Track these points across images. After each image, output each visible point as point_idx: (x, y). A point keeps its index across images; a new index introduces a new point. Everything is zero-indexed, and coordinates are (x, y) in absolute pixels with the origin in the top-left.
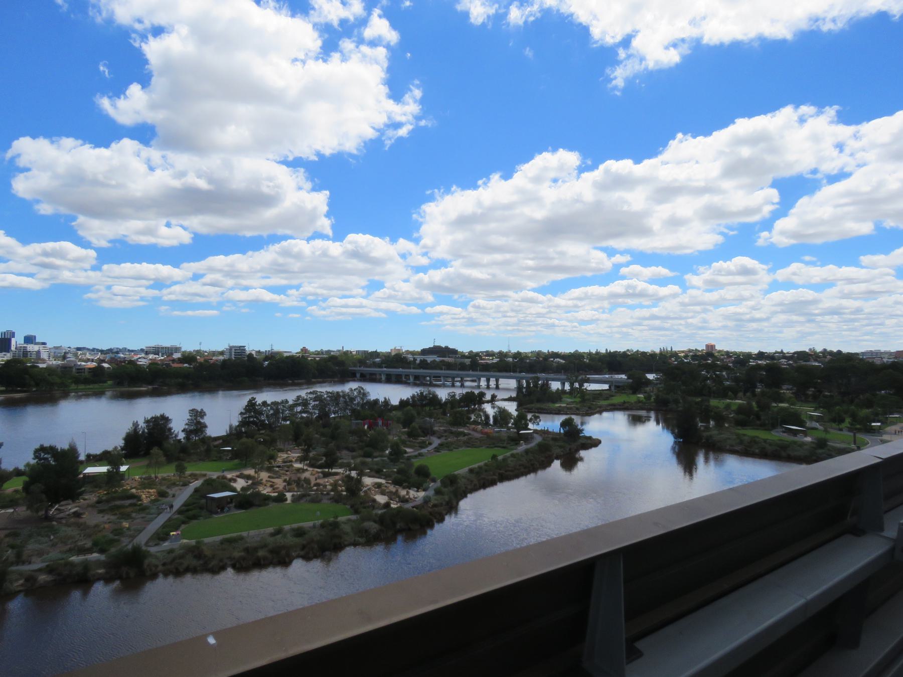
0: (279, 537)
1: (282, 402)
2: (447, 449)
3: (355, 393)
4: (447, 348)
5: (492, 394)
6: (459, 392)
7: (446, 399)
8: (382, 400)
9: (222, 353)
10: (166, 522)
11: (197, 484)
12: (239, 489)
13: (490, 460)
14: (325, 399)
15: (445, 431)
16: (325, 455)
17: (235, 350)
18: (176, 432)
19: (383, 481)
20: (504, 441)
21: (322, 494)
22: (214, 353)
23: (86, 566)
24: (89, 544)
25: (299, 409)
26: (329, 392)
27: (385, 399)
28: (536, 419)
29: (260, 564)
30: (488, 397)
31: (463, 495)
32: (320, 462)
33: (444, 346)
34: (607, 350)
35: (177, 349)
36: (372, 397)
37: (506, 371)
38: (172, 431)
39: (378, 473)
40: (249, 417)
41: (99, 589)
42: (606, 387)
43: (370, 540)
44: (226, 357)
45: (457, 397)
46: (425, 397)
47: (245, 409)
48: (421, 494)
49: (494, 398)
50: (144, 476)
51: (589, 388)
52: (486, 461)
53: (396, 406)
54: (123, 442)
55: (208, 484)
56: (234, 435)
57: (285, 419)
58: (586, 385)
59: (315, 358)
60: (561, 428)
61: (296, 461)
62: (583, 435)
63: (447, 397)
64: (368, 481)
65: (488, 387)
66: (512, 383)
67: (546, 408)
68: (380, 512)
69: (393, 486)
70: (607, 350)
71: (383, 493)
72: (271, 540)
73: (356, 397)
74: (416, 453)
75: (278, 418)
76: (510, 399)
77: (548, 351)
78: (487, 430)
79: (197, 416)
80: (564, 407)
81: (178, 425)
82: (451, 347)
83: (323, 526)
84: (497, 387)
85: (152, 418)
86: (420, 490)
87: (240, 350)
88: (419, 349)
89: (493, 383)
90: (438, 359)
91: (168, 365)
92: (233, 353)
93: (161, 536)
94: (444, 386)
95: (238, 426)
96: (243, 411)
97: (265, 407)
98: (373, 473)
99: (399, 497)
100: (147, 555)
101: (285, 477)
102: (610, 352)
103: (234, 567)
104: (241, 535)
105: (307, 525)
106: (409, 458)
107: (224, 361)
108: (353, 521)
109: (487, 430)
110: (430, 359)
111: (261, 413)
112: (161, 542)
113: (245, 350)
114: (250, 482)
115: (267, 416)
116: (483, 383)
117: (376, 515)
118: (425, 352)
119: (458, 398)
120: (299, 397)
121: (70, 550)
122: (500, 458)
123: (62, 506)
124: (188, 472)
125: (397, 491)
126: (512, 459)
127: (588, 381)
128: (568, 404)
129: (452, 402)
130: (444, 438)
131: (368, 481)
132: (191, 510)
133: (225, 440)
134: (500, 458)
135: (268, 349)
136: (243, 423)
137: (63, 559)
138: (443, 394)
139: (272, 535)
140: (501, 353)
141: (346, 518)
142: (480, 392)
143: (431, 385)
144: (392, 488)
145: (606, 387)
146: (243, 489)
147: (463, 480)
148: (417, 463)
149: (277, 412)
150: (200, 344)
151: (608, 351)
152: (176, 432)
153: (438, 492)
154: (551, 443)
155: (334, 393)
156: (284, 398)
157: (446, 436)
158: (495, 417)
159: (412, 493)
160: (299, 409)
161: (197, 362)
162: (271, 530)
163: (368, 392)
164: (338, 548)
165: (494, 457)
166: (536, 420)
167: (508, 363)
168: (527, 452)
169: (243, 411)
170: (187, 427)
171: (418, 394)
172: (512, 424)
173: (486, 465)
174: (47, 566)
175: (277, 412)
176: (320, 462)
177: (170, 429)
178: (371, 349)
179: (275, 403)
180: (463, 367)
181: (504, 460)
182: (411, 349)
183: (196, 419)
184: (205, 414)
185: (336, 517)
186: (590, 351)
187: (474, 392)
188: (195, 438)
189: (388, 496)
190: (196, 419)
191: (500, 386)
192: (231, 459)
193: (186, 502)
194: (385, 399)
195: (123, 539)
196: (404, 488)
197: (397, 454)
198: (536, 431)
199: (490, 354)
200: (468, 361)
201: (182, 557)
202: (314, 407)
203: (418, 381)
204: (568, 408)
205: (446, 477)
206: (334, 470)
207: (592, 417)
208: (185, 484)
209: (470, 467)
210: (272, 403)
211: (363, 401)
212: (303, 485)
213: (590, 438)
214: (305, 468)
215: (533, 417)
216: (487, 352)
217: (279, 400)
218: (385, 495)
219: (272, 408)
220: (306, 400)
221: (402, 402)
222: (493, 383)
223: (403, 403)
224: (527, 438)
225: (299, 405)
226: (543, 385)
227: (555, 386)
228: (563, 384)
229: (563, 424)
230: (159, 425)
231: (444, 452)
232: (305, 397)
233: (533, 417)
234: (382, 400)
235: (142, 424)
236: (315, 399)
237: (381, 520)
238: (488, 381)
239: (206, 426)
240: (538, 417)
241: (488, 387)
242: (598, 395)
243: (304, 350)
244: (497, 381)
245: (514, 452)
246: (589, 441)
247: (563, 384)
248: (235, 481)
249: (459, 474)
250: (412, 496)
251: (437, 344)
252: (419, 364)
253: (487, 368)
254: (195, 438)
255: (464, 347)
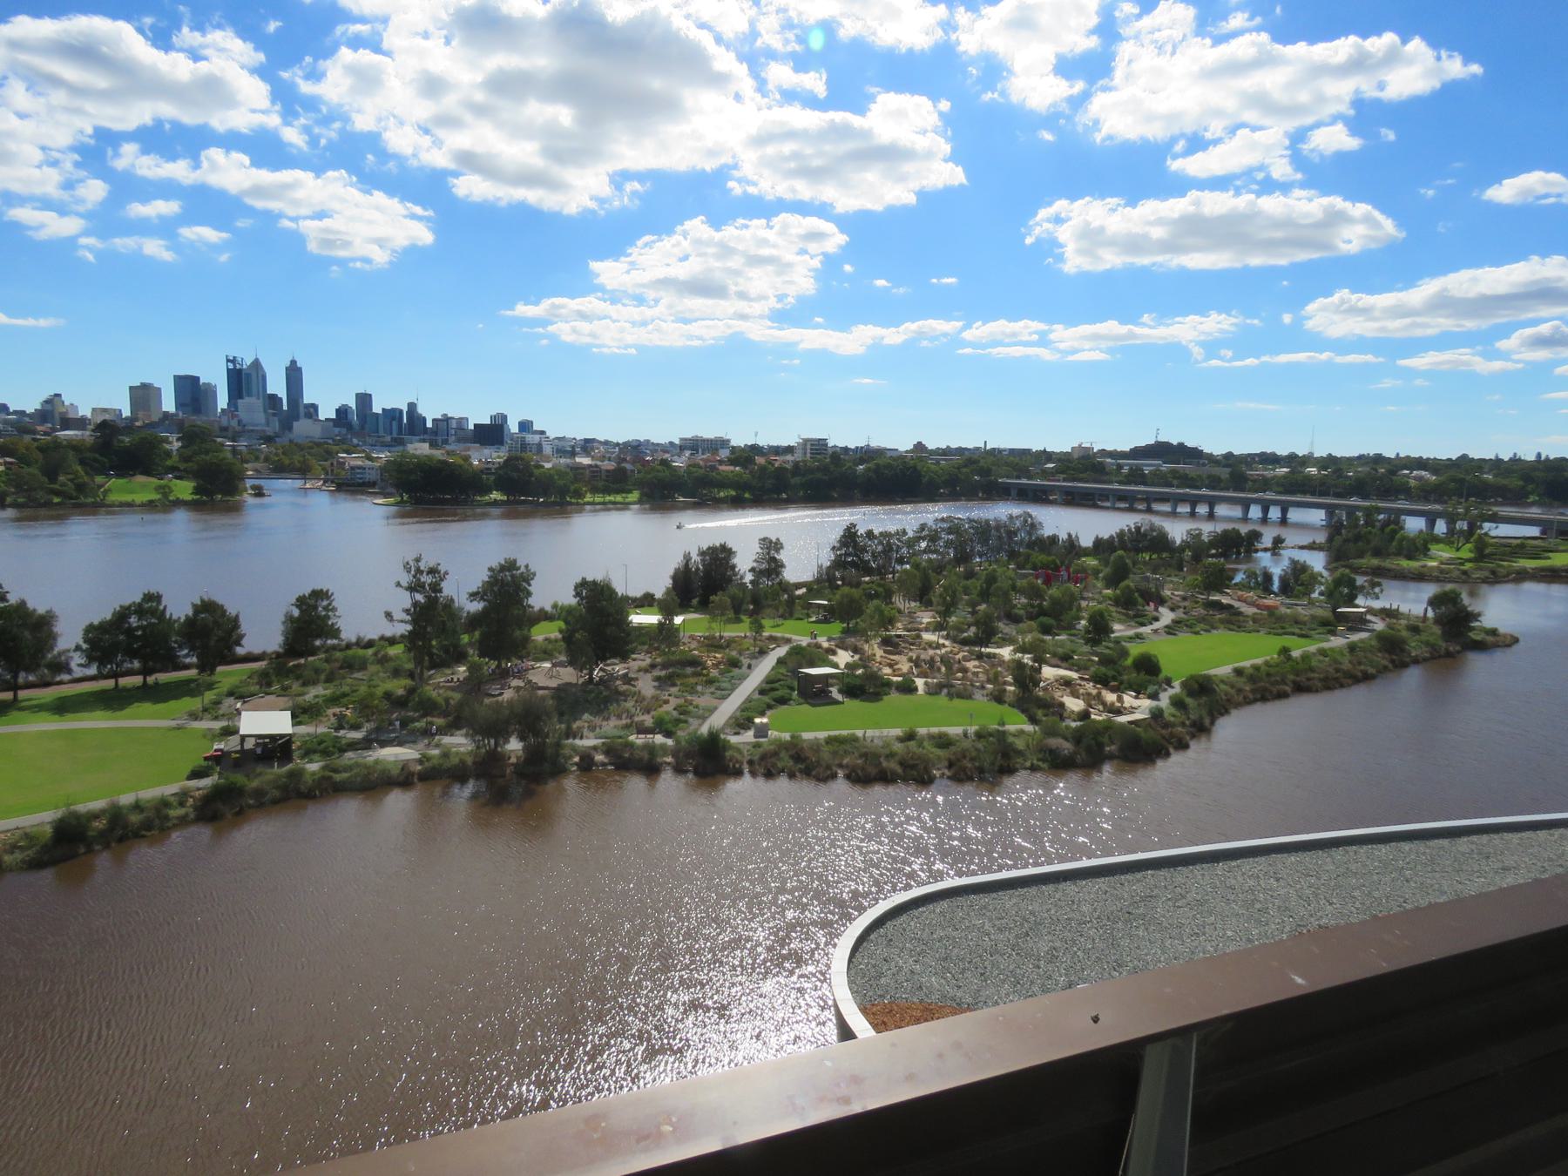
0: (912, 744)
1: (897, 533)
2: (1188, 630)
3: (1018, 524)
4: (1181, 445)
5: (1275, 535)
6: (1207, 529)
7: (1183, 541)
8: (1063, 536)
9: (789, 450)
10: (744, 702)
11: (782, 651)
12: (842, 666)
13: (1276, 656)
14: (966, 530)
15: (1184, 599)
16: (976, 624)
17: (812, 445)
18: (742, 572)
19: (1074, 675)
20: (1304, 623)
21: (972, 685)
22: (778, 451)
23: (651, 749)
24: (648, 720)
25: (923, 545)
26: (973, 521)
27: (1070, 535)
28: (1371, 590)
29: (886, 778)
30: (1267, 541)
31: (1223, 711)
32: (966, 634)
33: (1175, 443)
34: (1539, 455)
35: (723, 443)
36: (1047, 532)
37: (1304, 493)
38: (737, 570)
39: (1065, 660)
40: (846, 555)
41: (669, 782)
42: (1534, 531)
43: (1058, 764)
44: (798, 456)
45: (1205, 538)
46: (1145, 535)
47: (840, 541)
48: (1146, 703)
49: (1278, 542)
50: (707, 634)
51: (1493, 533)
52: (1268, 658)
53: (1086, 549)
54: (671, 582)
55: (797, 654)
56: (825, 581)
57: (901, 561)
58: (1487, 525)
59: (938, 462)
60: (1429, 609)
61: (927, 630)
62: (1477, 624)
63: (1185, 538)
64: (1048, 672)
65: (1264, 520)
66: (1317, 516)
67: (1393, 567)
68: (1074, 725)
69: (1091, 684)
70: (1539, 455)
71: (1075, 695)
72: (898, 747)
73: (1018, 529)
74: (1131, 633)
75: (890, 559)
76: (1312, 547)
77: (1398, 454)
78: (1270, 601)
79: (771, 547)
80: (1432, 567)
81: (745, 562)
82: (1190, 444)
83: (980, 735)
84: (1284, 521)
85: (709, 548)
86: (1141, 696)
87: (818, 446)
88: (1127, 449)
89: (1275, 513)
90: (1165, 467)
91: (713, 468)
92: (809, 451)
93: (742, 722)
94: (1173, 514)
95: (829, 568)
96: (837, 545)
97: (870, 539)
98: (1055, 661)
99: (1104, 704)
100: (726, 746)
101: (910, 654)
102: (1547, 459)
103: (848, 777)
104: (854, 734)
105: (954, 731)
106: (1117, 641)
107: (796, 464)
108: (1028, 734)
109: (1270, 601)
110: (1148, 466)
111: (864, 550)
112: (742, 731)
113: (827, 445)
114: (857, 657)
115: (873, 555)
116: (1255, 512)
117: (1067, 727)
118: (1137, 453)
119: (1206, 540)
120: (923, 527)
121: (627, 727)
122: (1296, 654)
123: (608, 665)
124: (766, 634)
125: (1099, 694)
126: (1321, 658)
127: (1495, 519)
128: (1442, 563)
129: (1196, 547)
130: (1182, 610)
131: (1048, 672)
132: (777, 690)
133: (814, 588)
134: (1296, 654)
135: (862, 444)
136: (838, 564)
137: (620, 737)
138: (1177, 531)
139: (901, 740)
140: (1292, 459)
141: (1018, 725)
142: (1250, 531)
143: (1149, 510)
144: (1090, 687)
145: (1534, 531)
146: (848, 666)
147: (1223, 687)
148: (1135, 650)
149: (888, 549)
150: (756, 434)
151: (1543, 458)
152: (742, 572)
153: (1177, 703)
154: (1405, 634)
155: (980, 523)
156: (900, 527)
157: (1185, 608)
158: (1283, 580)
159: (1129, 699)
160: (923, 545)
161: (755, 464)
162: (898, 732)
163: (1040, 523)
164: (1009, 770)
165: (1285, 651)
166: (1373, 588)
167: (1309, 477)
168: (1352, 648)
169: (837, 545)
170: (755, 564)
171: (1130, 530)
172: (1321, 594)
173: (1267, 663)
174: (603, 743)
175: (888, 549)
176: (966, 634)
177: (734, 567)
178: (1036, 446)
179: (885, 535)
180: (1214, 483)
181: (1305, 657)
182: (1109, 448)
183: (768, 553)
184: (782, 548)
185: (1003, 724)
186: (1497, 457)
187: (1238, 531)
188: (766, 582)
189: (1083, 700)
190: (768, 553)
191: (1289, 521)
192: (826, 621)
193: (766, 677)
194: (1070, 535)
195: (691, 720)
196: (1113, 690)
197: (1099, 629)
198: (1371, 611)
199: (1270, 459)
200: (1224, 473)
201: (775, 754)
202: (948, 544)
203: (1128, 502)
204: (1442, 571)
205: (1193, 678)
206: (988, 650)
207: (1498, 587)
208: (763, 652)
209: (1236, 665)
210: (881, 533)
211: (1031, 537)
212: (939, 669)
213: (1494, 632)
214: (941, 641)
215: (1366, 584)
216: (1263, 454)
217: (892, 528)
218: (1078, 698)
219: (881, 543)
220: (936, 531)
221: (1098, 543)
222: (1275, 513)
223: (1101, 547)
224: (1357, 623)
225: (924, 539)
226: (1387, 523)
227: (1414, 525)
228: (1431, 524)
229: (1434, 602)
230: (719, 558)
231: (1185, 638)
232: (934, 527)
233: (1366, 584)
234: (1063, 536)
235: (695, 557)
236: (950, 531)
237: (1077, 737)
238: (1265, 510)
239: (783, 566)
240: (1379, 584)
241: (1264, 520)
242: (1520, 548)
243: (919, 447)
244: (1284, 512)
245: (1325, 645)
246: (1490, 639)
247: (1431, 524)
248: (834, 653)
249: (1215, 676)
250: (1126, 705)
251: (1162, 439)
252: (1127, 476)
253: (1265, 484)
254: (766, 582)
255: (1215, 446)
